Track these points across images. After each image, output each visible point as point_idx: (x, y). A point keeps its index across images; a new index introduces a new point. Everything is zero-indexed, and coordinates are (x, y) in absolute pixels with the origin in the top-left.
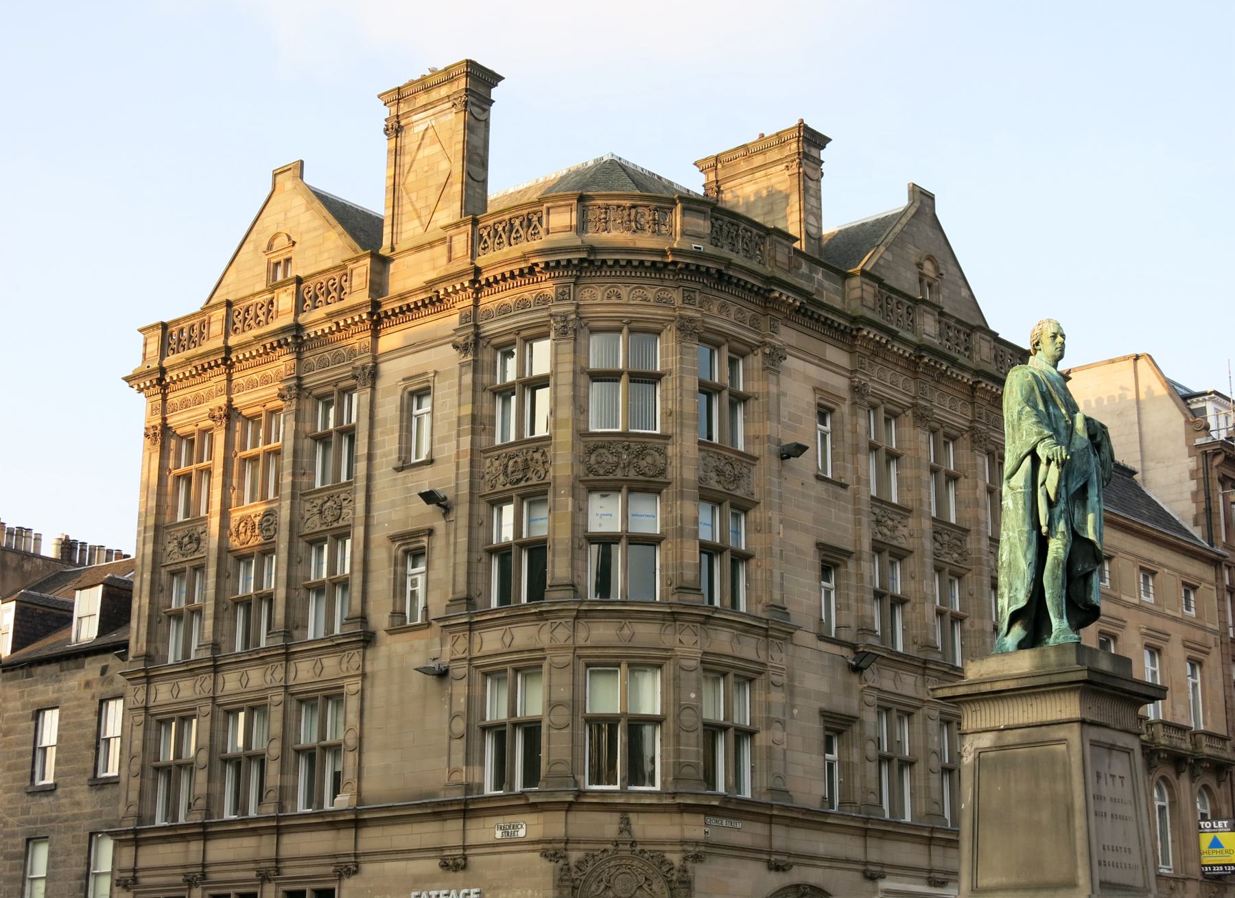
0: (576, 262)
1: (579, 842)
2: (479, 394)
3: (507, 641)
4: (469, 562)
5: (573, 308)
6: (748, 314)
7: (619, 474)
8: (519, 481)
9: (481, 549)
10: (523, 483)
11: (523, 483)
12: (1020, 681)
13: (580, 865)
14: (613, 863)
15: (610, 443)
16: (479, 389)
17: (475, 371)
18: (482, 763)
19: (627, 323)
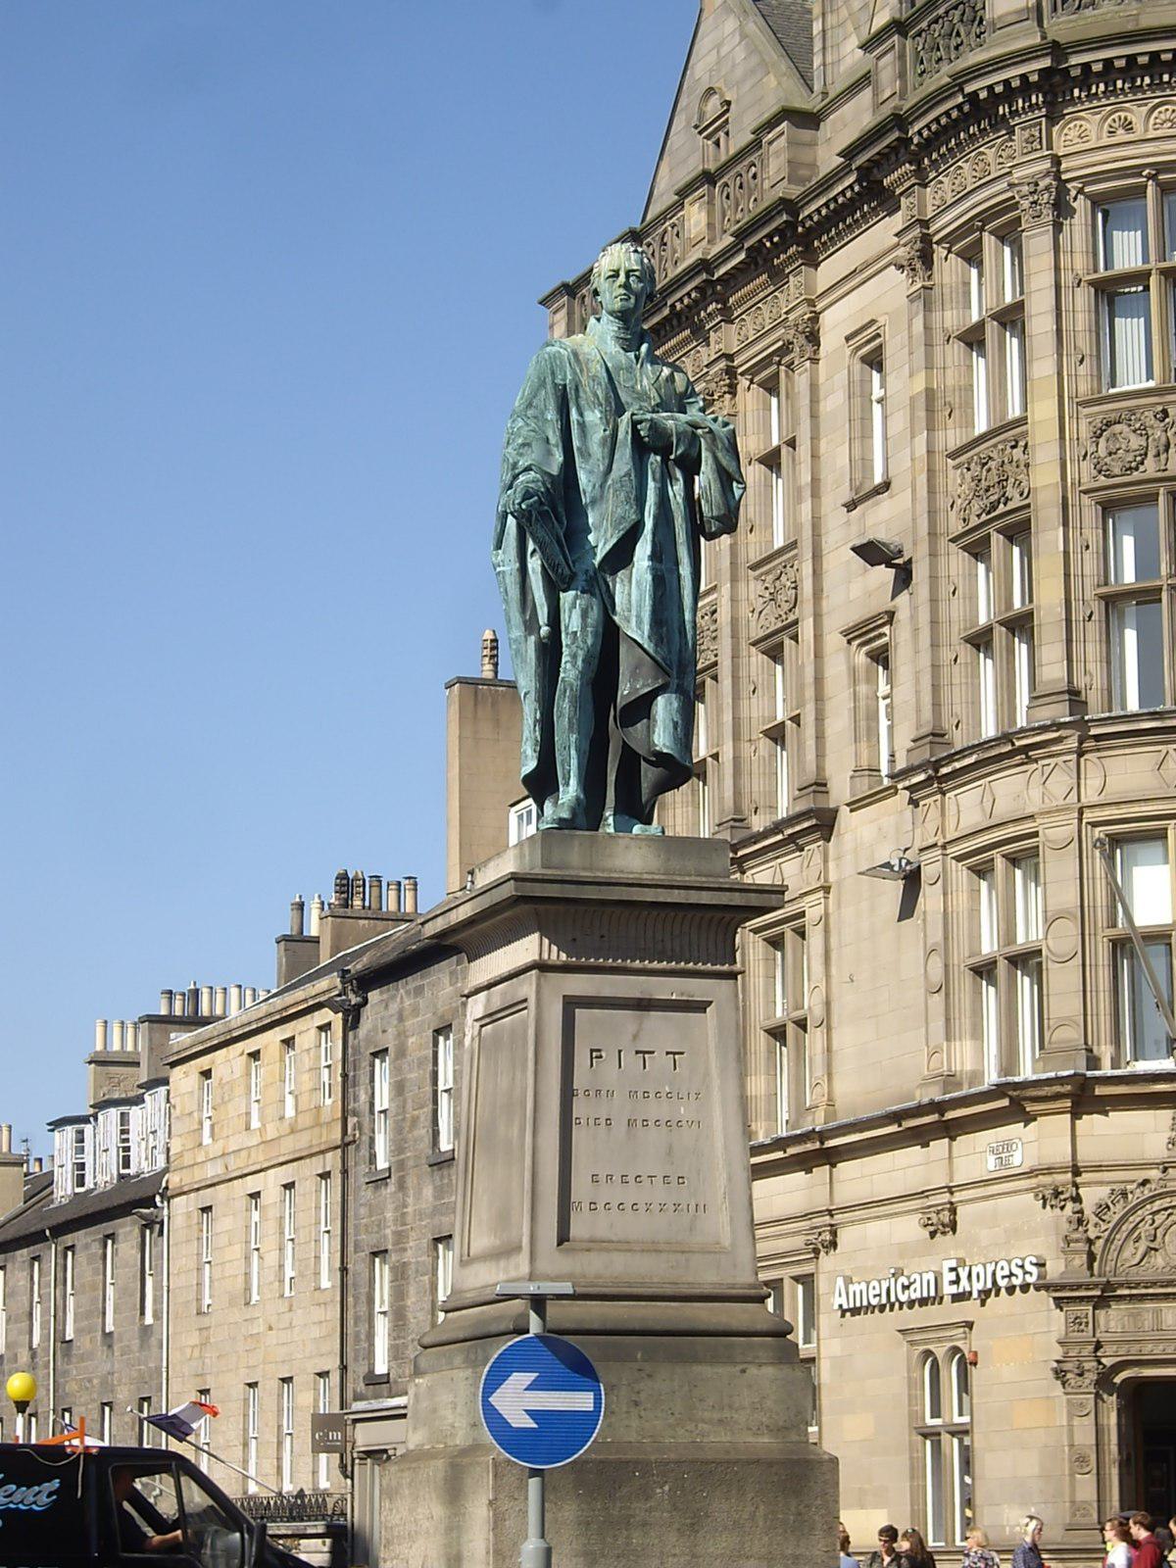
0: (1034, 78)
1: (1098, 1168)
2: (938, 350)
3: (988, 805)
4: (935, 667)
5: (1047, 165)
7: (1150, 468)
8: (994, 507)
9: (956, 638)
10: (1001, 509)
11: (1001, 509)
13: (1103, 1208)
14: (1157, 1205)
15: (1132, 411)
16: (938, 338)
17: (928, 308)
18: (977, 1033)
19: (1150, 177)
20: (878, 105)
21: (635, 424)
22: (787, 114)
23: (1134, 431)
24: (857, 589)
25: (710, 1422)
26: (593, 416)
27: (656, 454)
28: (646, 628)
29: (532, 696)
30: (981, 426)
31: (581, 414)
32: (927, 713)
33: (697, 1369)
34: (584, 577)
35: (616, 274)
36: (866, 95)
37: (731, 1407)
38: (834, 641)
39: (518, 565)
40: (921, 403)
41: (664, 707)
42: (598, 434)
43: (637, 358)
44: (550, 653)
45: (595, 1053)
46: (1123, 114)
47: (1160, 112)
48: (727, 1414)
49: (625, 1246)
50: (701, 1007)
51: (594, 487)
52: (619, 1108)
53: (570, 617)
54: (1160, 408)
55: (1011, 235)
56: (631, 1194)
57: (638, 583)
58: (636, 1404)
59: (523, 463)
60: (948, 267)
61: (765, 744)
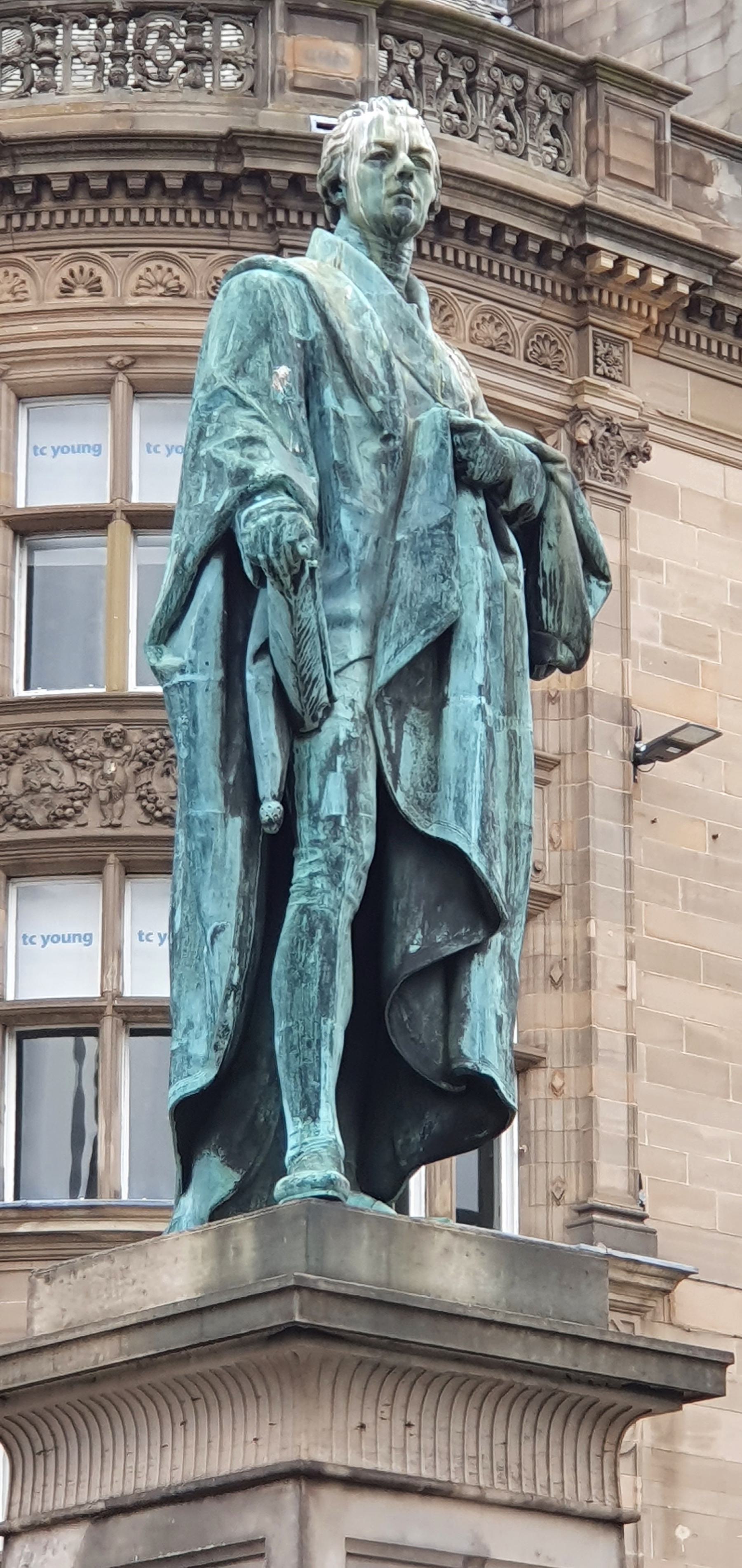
6: (521, 326)
7: (92, 822)
12: (126, 1341)
15: (70, 727)
19: (122, 368)
23: (72, 760)
27: (476, 494)
29: (229, 936)
34: (349, 714)
39: (220, 674)
46: (87, 266)
47: (160, 267)
51: (365, 543)
53: (322, 787)
54: (117, 727)
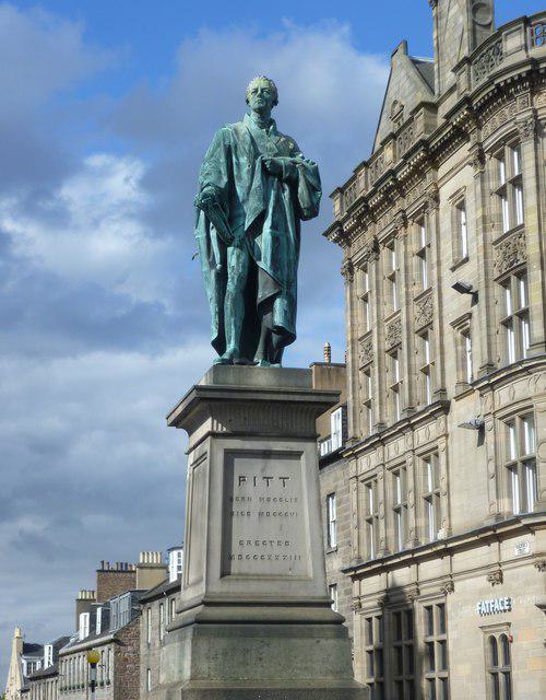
2: (487, 199)
4: (489, 335)
8: (512, 264)
9: (497, 323)
16: (487, 193)
17: (482, 181)
18: (510, 495)
20: (459, 95)
21: (263, 162)
22: (423, 104)
24: (456, 304)
25: (300, 669)
26: (244, 160)
28: (269, 263)
29: (214, 300)
30: (507, 228)
31: (237, 159)
32: (486, 356)
33: (293, 641)
35: (256, 91)
36: (455, 95)
37: (311, 660)
38: (447, 327)
40: (480, 222)
41: (279, 304)
42: (245, 169)
43: (267, 132)
44: (222, 277)
45: (242, 479)
48: (309, 664)
49: (259, 577)
50: (297, 455)
52: (255, 506)
55: (516, 146)
56: (259, 551)
57: (265, 241)
58: (260, 659)
59: (206, 182)
60: (491, 163)
61: (421, 375)
